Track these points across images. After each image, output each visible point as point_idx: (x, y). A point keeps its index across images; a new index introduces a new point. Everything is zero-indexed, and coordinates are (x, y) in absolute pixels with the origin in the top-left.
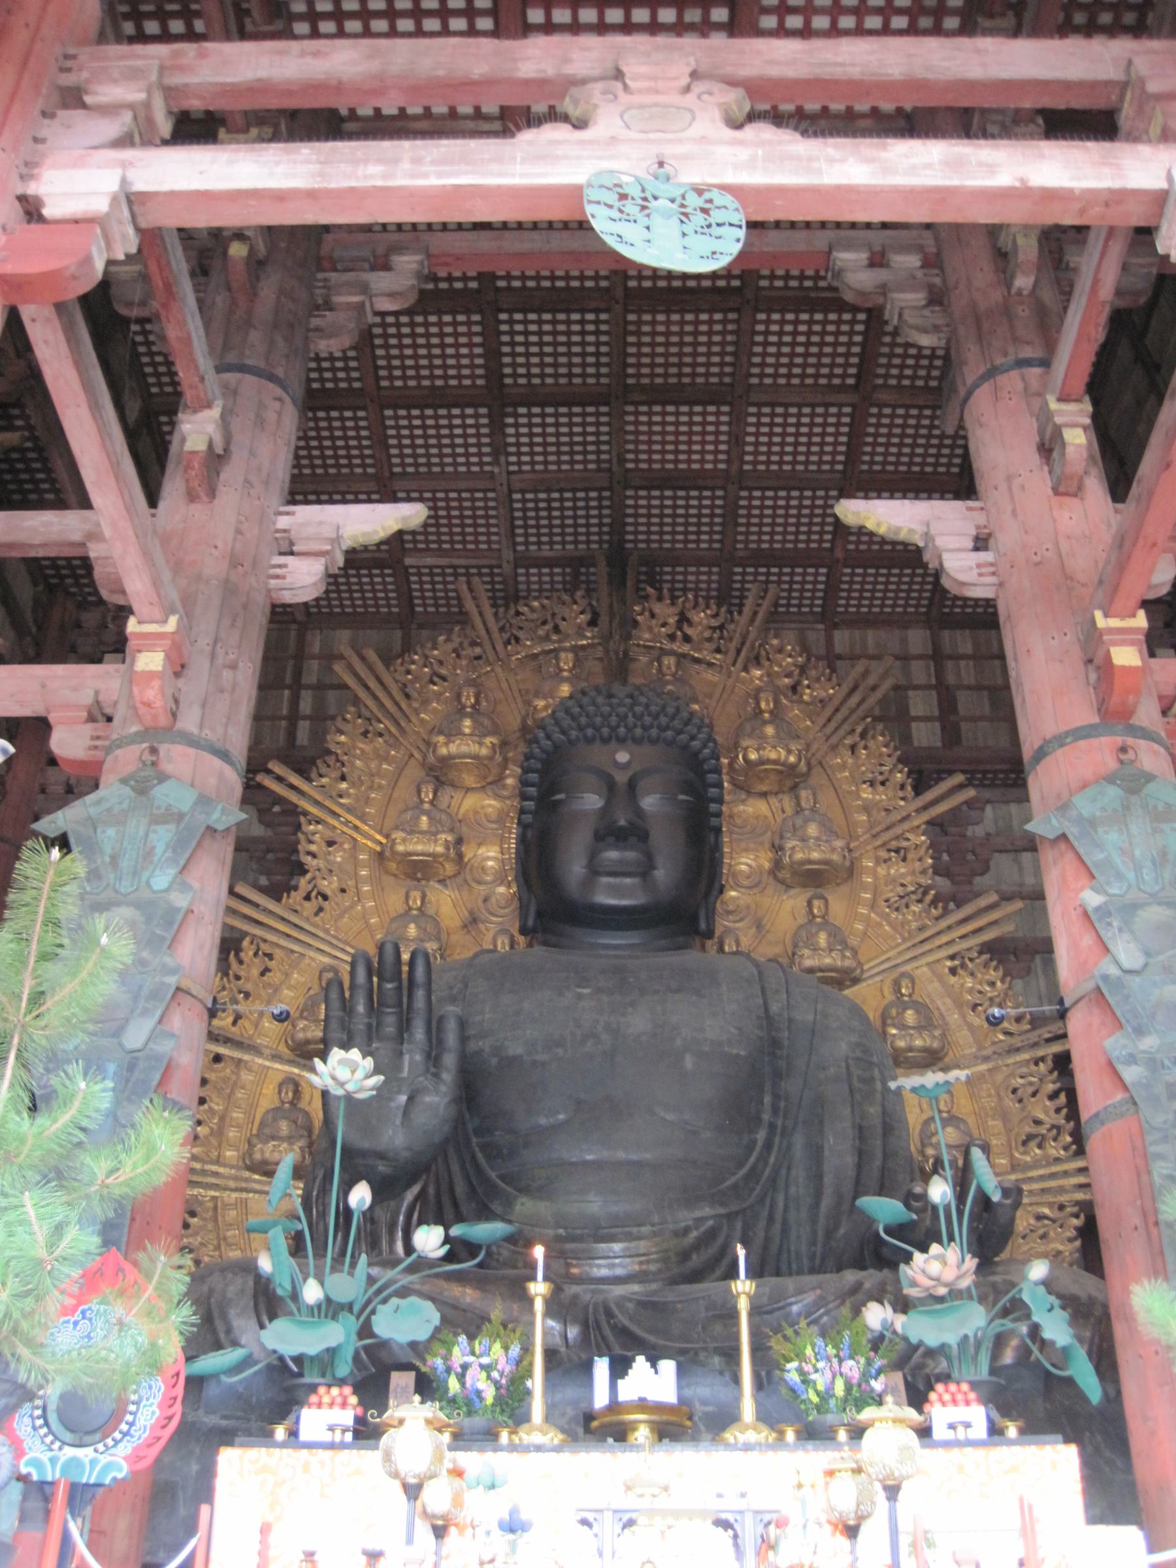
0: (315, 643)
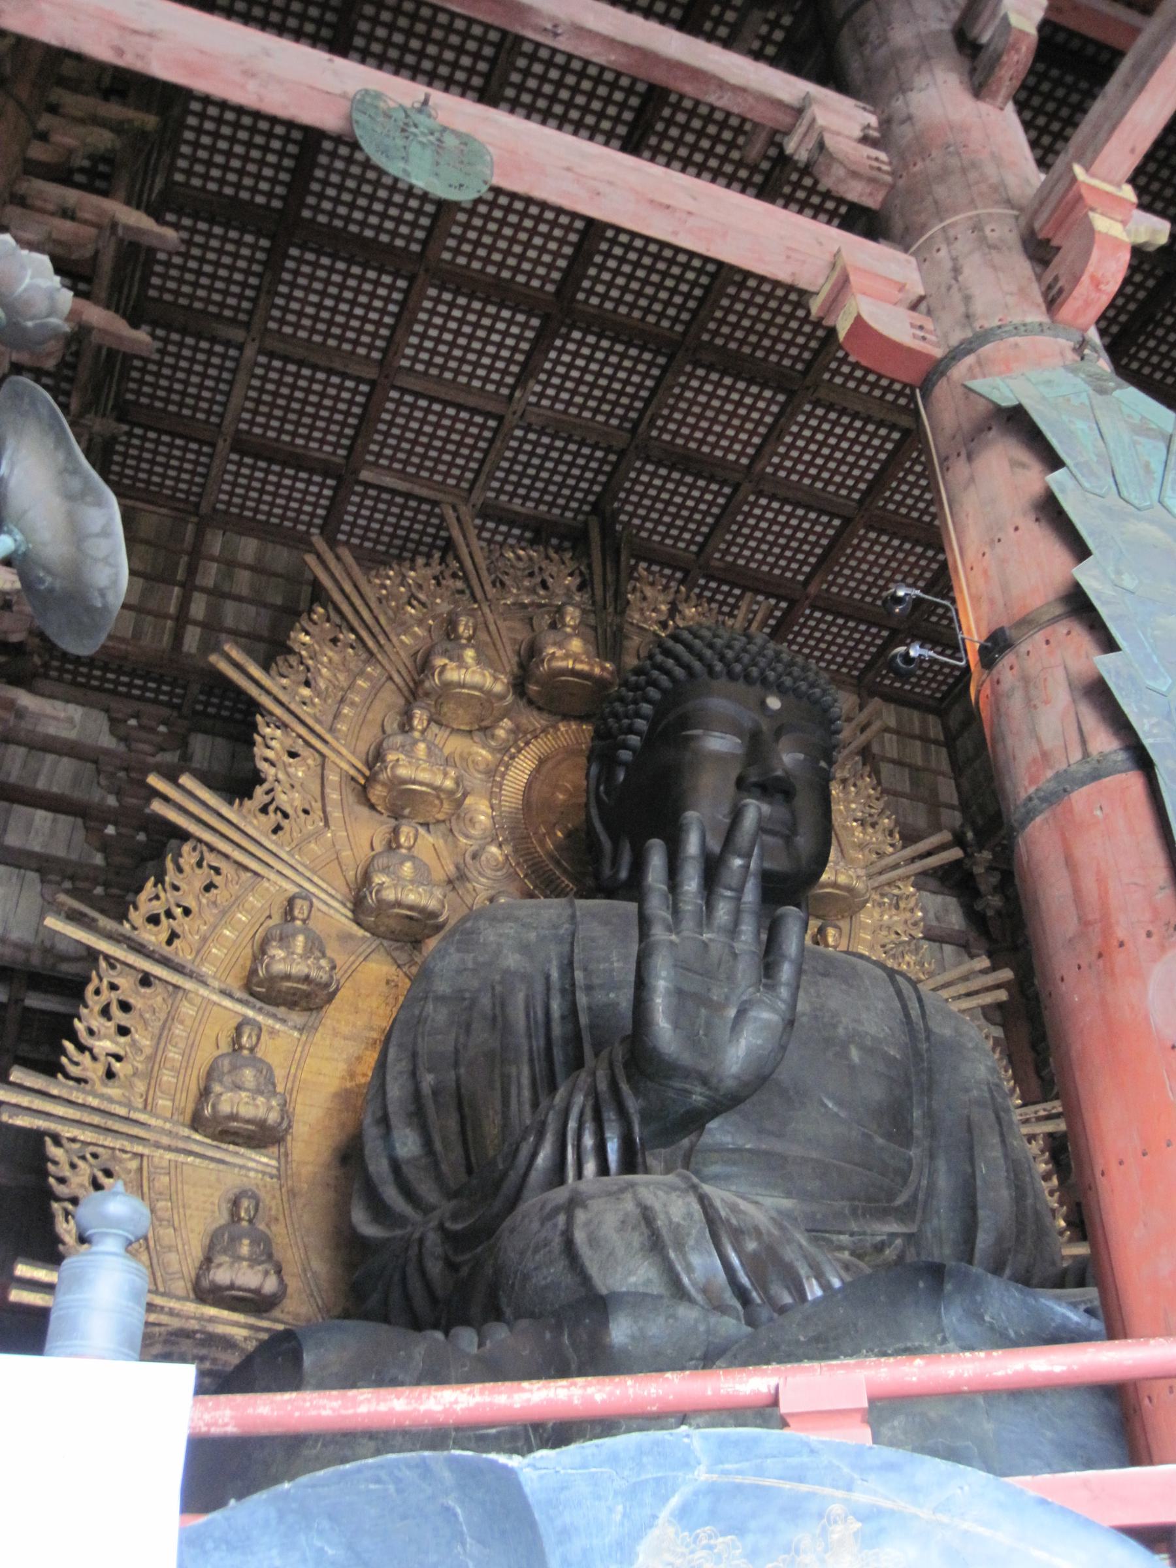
0: (216, 543)
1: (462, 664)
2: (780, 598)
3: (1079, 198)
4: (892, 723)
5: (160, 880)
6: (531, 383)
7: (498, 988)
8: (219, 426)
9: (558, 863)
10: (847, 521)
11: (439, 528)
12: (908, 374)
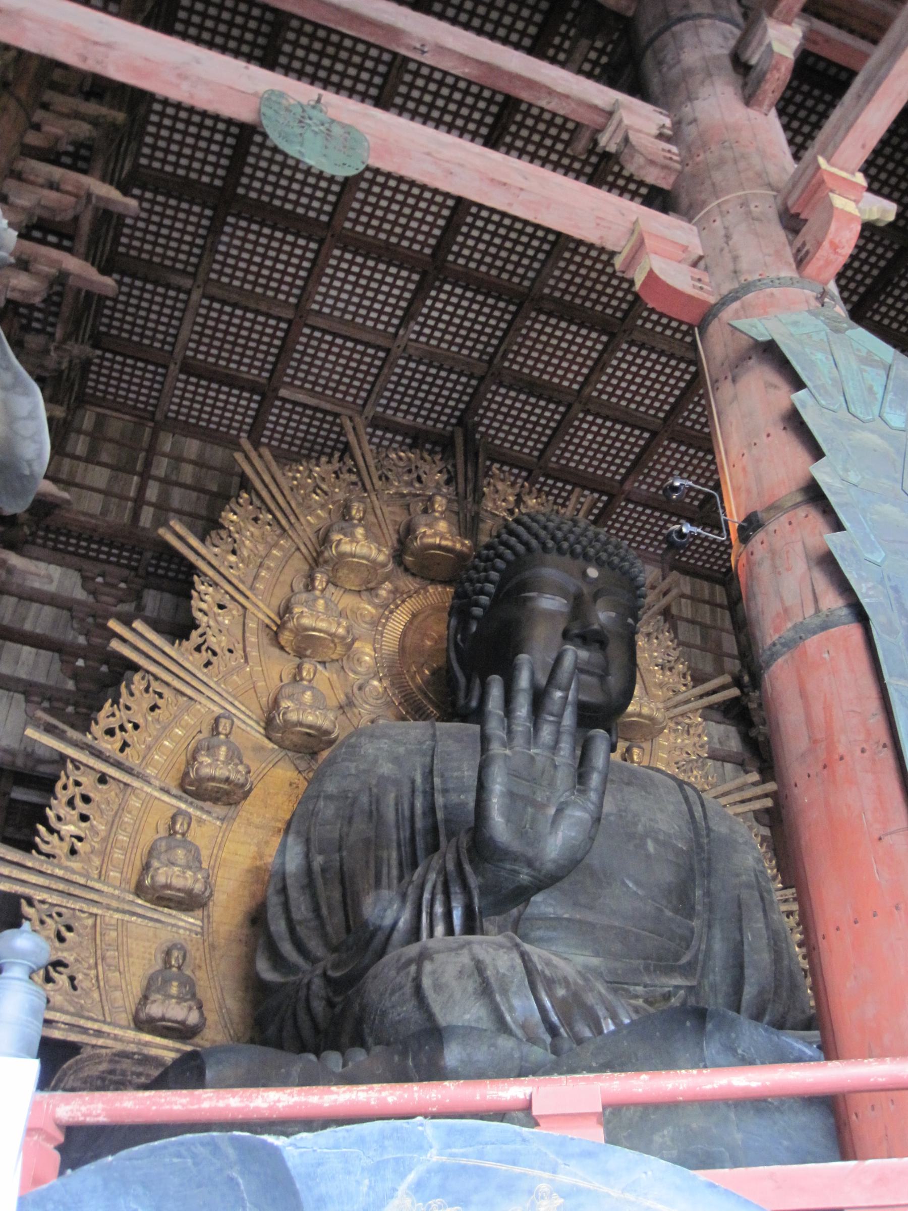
0: (167, 443)
1: (354, 540)
2: (602, 493)
3: (822, 182)
4: (687, 590)
5: (116, 702)
6: (412, 323)
7: (375, 790)
8: (172, 352)
9: (425, 695)
10: (654, 434)
11: (340, 434)
12: (690, 316)
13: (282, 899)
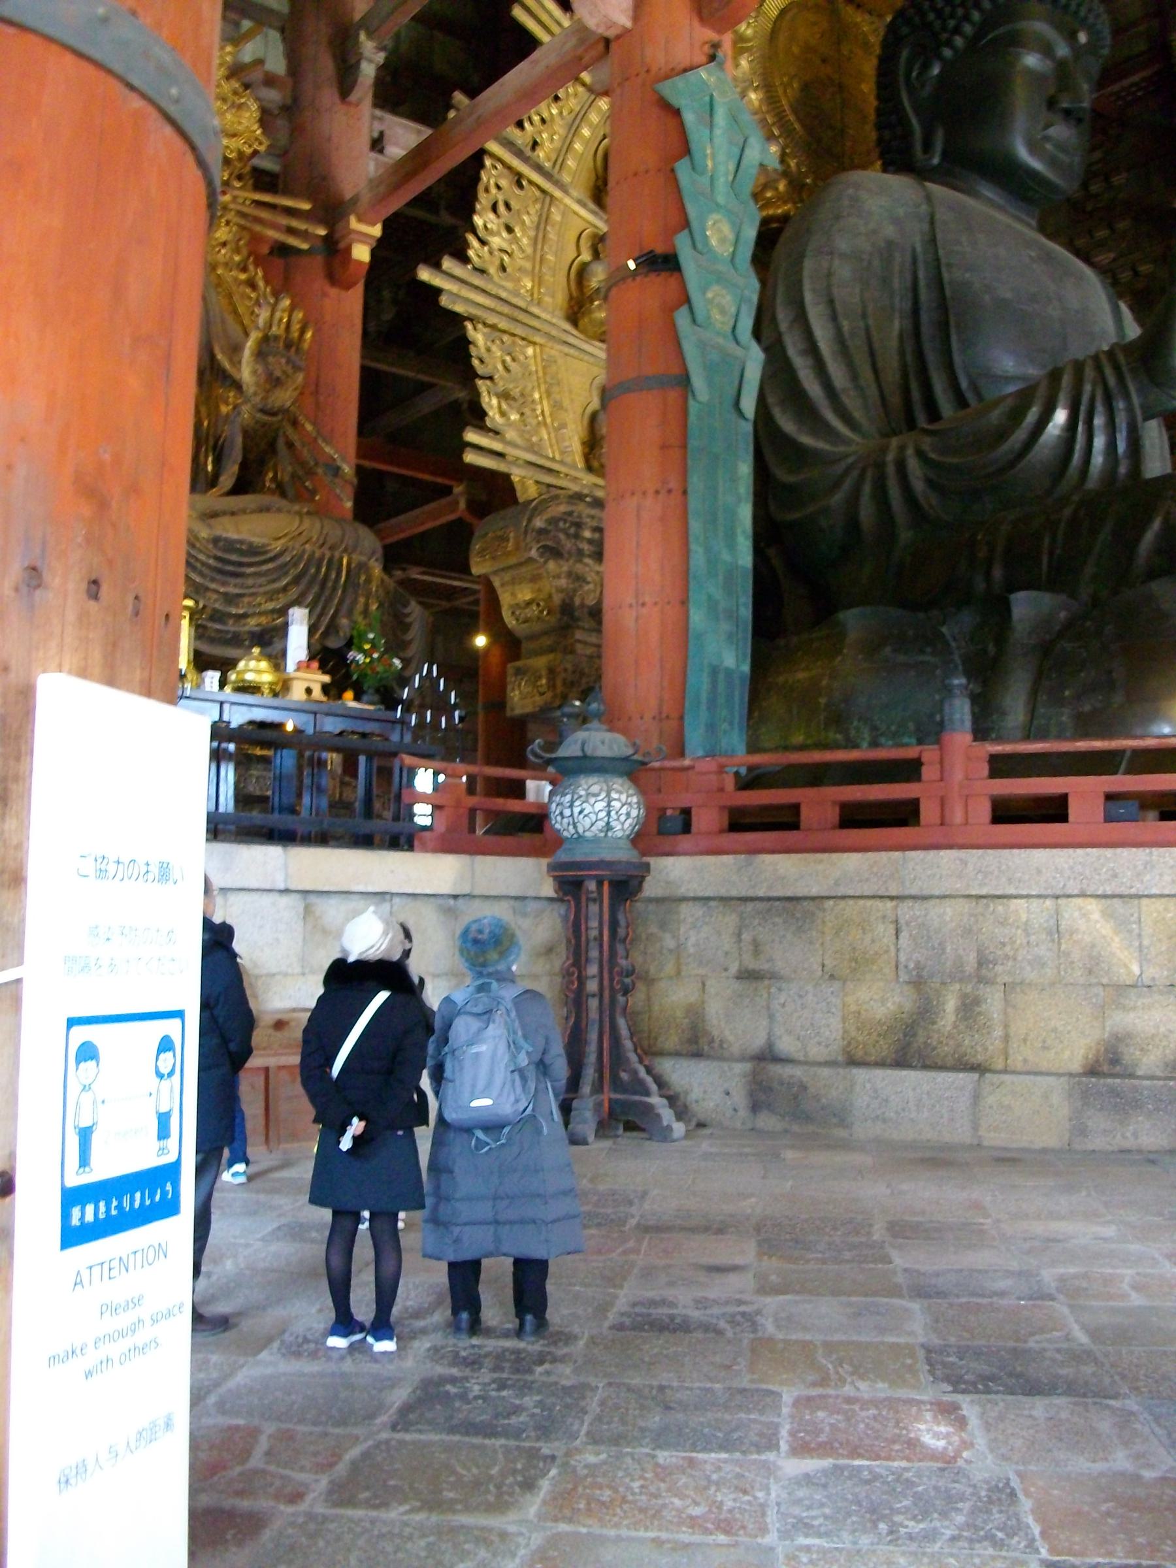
13: (809, 362)
